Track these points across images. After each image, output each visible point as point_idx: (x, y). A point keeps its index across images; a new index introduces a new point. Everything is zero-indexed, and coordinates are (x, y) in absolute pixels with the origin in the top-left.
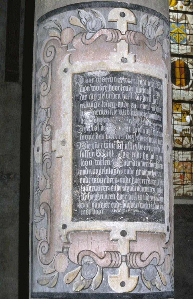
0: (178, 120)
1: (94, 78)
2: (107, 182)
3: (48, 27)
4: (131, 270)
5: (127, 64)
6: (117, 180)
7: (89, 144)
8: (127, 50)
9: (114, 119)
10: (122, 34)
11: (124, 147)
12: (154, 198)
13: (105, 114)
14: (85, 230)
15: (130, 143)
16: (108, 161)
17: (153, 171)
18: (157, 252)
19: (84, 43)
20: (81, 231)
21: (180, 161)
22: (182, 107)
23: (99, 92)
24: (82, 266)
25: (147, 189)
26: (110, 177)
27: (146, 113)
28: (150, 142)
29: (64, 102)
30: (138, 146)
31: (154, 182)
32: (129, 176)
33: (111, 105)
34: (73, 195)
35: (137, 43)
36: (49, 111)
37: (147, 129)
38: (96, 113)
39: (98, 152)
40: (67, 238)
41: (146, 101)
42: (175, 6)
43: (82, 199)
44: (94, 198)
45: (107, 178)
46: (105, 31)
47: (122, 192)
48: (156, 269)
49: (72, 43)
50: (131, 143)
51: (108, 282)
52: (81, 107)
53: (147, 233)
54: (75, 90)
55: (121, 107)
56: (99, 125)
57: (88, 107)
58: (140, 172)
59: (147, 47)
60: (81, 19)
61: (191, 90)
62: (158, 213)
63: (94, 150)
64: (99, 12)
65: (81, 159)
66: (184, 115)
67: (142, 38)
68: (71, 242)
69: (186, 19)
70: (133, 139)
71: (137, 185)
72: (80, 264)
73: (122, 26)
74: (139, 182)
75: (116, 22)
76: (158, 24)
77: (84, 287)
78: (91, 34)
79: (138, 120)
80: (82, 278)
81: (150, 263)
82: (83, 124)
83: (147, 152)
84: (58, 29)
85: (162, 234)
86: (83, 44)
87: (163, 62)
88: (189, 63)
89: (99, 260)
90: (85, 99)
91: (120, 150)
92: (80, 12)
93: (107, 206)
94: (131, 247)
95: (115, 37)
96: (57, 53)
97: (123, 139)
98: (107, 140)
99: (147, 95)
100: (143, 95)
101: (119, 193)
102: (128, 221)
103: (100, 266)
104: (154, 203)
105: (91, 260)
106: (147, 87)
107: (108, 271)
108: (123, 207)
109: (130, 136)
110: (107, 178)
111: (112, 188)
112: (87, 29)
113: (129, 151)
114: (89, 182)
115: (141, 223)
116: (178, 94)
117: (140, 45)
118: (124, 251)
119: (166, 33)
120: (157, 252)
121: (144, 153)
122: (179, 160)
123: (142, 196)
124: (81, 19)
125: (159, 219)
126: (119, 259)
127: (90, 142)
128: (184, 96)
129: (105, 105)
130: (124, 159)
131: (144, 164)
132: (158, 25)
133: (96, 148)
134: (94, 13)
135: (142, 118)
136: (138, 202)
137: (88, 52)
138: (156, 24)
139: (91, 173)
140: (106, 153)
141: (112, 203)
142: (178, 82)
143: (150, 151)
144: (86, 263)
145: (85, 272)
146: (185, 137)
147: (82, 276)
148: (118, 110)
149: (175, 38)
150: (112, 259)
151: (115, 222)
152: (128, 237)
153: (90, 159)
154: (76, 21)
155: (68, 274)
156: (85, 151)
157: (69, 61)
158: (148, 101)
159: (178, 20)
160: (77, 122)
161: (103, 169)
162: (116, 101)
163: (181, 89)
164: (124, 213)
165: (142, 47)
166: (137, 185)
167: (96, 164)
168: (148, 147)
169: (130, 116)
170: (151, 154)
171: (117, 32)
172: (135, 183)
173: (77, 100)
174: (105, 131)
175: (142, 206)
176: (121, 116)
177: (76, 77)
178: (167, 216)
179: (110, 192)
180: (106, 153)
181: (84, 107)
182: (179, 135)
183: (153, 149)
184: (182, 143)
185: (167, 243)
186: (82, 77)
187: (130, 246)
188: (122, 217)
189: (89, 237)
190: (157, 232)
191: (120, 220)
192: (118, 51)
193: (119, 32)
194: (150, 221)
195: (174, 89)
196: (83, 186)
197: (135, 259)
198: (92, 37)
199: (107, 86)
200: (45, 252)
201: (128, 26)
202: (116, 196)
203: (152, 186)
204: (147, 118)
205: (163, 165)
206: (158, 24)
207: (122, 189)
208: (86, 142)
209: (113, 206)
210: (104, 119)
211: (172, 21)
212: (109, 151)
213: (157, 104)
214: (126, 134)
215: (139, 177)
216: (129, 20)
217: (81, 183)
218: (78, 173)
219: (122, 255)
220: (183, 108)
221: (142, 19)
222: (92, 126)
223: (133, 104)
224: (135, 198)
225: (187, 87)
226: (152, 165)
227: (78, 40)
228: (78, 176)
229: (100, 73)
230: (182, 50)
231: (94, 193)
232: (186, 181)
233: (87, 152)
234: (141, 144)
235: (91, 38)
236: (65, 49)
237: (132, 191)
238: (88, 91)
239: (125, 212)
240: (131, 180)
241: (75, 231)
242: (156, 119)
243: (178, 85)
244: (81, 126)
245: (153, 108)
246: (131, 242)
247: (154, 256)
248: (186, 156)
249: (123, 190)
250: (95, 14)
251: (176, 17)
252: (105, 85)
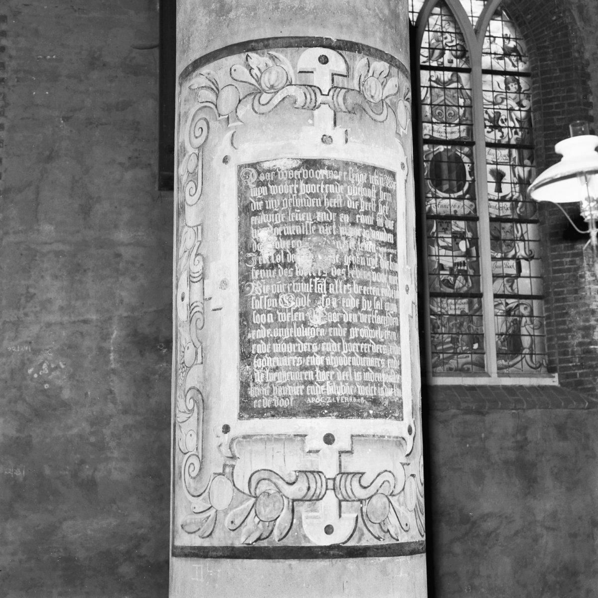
0: (445, 248)
1: (275, 172)
2: (299, 351)
3: (195, 86)
4: (343, 503)
5: (332, 145)
6: (316, 347)
7: (268, 286)
8: (333, 122)
9: (311, 241)
10: (323, 93)
11: (328, 289)
12: (383, 377)
13: (294, 234)
14: (261, 435)
15: (338, 283)
16: (300, 314)
17: (381, 330)
18: (390, 472)
19: (256, 112)
20: (255, 435)
21: (451, 315)
22: (453, 227)
23: (284, 195)
24: (256, 497)
25: (371, 362)
26: (304, 342)
27: (367, 231)
28: (374, 280)
29: (225, 215)
30: (352, 287)
31: (382, 348)
32: (337, 339)
33: (305, 218)
34: (242, 374)
35: (350, 109)
36: (200, 231)
37: (369, 257)
38: (279, 231)
39: (282, 299)
40: (230, 448)
41: (366, 209)
42: (439, 60)
43: (256, 381)
44: (276, 378)
45: (298, 343)
46: (291, 90)
47: (326, 368)
48: (390, 502)
49: (236, 112)
50: (341, 283)
51: (302, 527)
52: (254, 222)
53: (371, 438)
54: (242, 193)
55: (323, 220)
56: (284, 252)
57: (265, 221)
58: (356, 332)
59: (368, 116)
60: (251, 69)
61: (467, 199)
62: (390, 402)
63: (277, 296)
64: (281, 56)
65: (255, 311)
66: (455, 240)
67: (359, 99)
68: (238, 456)
69: (459, 80)
70: (343, 275)
71: (353, 354)
72: (253, 494)
73: (322, 79)
74: (355, 349)
75: (312, 72)
76: (389, 75)
77: (261, 535)
78: (270, 96)
79: (353, 243)
80: (257, 520)
81: (378, 491)
82: (257, 251)
83: (369, 297)
84: (212, 89)
85: (399, 439)
86: (254, 114)
87: (397, 141)
88: (463, 154)
89: (286, 487)
90: (260, 209)
91: (321, 295)
92: (248, 58)
93: (299, 392)
94: (342, 464)
95: (311, 99)
96: (211, 130)
97: (326, 275)
98: (298, 278)
99: (369, 200)
100: (362, 200)
101: (321, 369)
102: (337, 417)
103: (288, 498)
104: (384, 385)
105: (272, 486)
106: (368, 185)
107: (302, 506)
108: (328, 394)
109: (339, 270)
110: (298, 343)
111: (308, 361)
112: (261, 87)
113: (337, 296)
114: (268, 351)
115: (360, 420)
116: (445, 206)
117: (354, 113)
118: (331, 471)
119: (404, 92)
120: (390, 472)
121: (364, 300)
122: (449, 313)
123: (360, 373)
124: (251, 69)
125: (393, 412)
126: (322, 485)
127: (268, 281)
128: (456, 209)
129: (294, 218)
130: (328, 311)
131: (364, 318)
132: (388, 78)
133: (278, 292)
134: (273, 58)
135: (361, 239)
136: (355, 385)
137: (264, 127)
138: (384, 75)
139: (271, 335)
140: (296, 301)
141: (308, 387)
142: (446, 186)
143: (375, 295)
144: (264, 492)
145: (262, 508)
147: (256, 515)
148: (316, 226)
149: (439, 113)
150: (309, 484)
151: (314, 419)
152: (338, 445)
153: (269, 312)
154: (242, 73)
155: (232, 512)
156: (261, 297)
157: (232, 143)
158: (371, 209)
159: (444, 83)
160: (246, 247)
161: (292, 329)
162: (314, 210)
163: (450, 198)
164: (329, 403)
165: (358, 116)
166: (353, 354)
167: (279, 320)
168: (371, 288)
169: (338, 237)
170: (376, 301)
171: (314, 91)
172: (349, 352)
173: (246, 210)
174: (295, 262)
175: (364, 391)
176: (323, 235)
177: (244, 170)
178: (407, 409)
179: (304, 368)
180: (296, 301)
181: (257, 222)
182: (448, 273)
183: (380, 293)
184: (454, 285)
185: (408, 455)
186: (253, 171)
187: (340, 462)
188: (326, 411)
189: (269, 446)
190: (389, 437)
191: (322, 416)
192: (316, 123)
193: (317, 91)
194: (376, 416)
195: (439, 198)
196: (257, 358)
197: (351, 485)
198: (270, 100)
199: (297, 186)
200: (194, 474)
201: (333, 80)
202: (315, 374)
203: (378, 355)
204: (368, 239)
205: (399, 318)
206: (387, 76)
207: (325, 361)
208: (262, 283)
209: (310, 392)
210: (292, 242)
211: (435, 85)
212: (301, 296)
213: (387, 214)
214: (331, 268)
215: (355, 340)
216: (336, 70)
217: (253, 352)
218: (249, 336)
219: (327, 477)
220: (455, 228)
221: (358, 67)
222: (272, 254)
223: (343, 214)
224: (349, 378)
225: (461, 193)
226: (379, 320)
227: (246, 106)
228: (249, 341)
229: (284, 164)
230: (452, 133)
231: (276, 369)
232: (462, 347)
233: (263, 299)
234: (359, 284)
235: (268, 103)
236: (224, 124)
237: (343, 366)
238: (264, 194)
239: (331, 401)
240: (341, 346)
241: (244, 437)
242: (385, 241)
243: (446, 192)
244: (254, 255)
245: (380, 222)
246: (343, 455)
247: (385, 479)
248: (462, 306)
249: (327, 364)
250: (276, 59)
251: (442, 79)
252: (294, 184)
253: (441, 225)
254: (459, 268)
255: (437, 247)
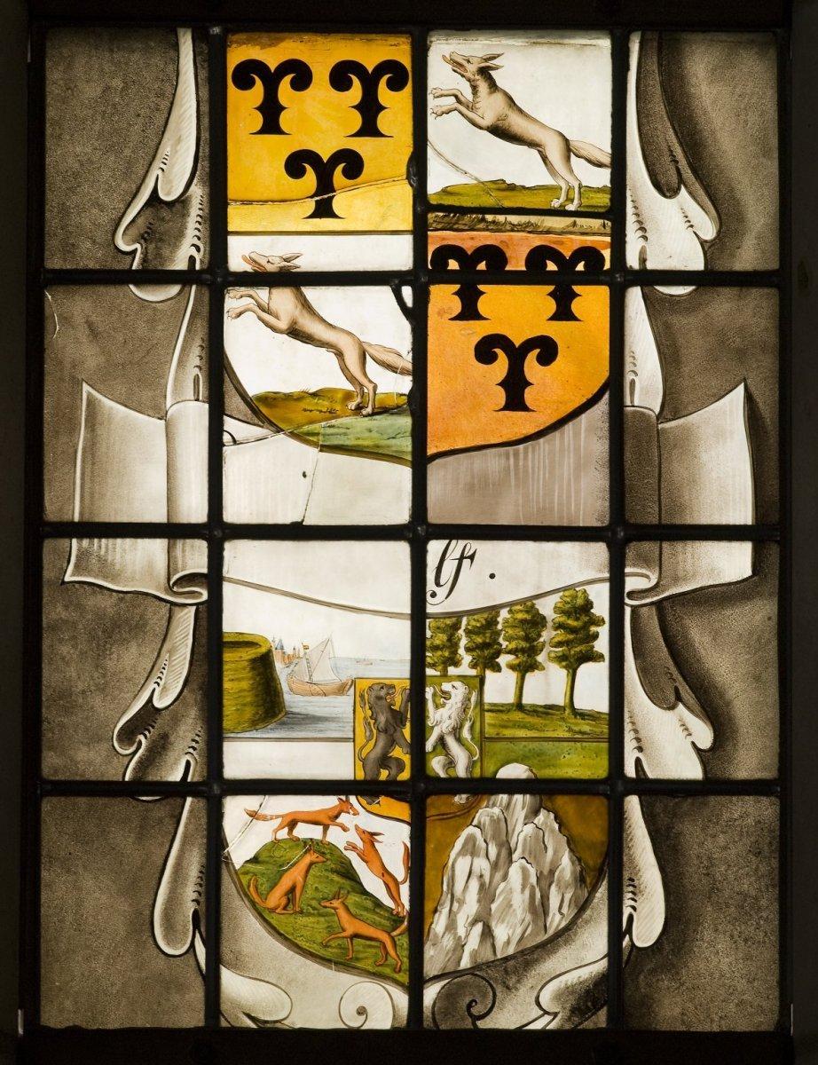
146: (484, 787)
182: (339, 763)
220: (464, 159)
253: (271, 118)
254: (499, 687)
255: (193, 416)
